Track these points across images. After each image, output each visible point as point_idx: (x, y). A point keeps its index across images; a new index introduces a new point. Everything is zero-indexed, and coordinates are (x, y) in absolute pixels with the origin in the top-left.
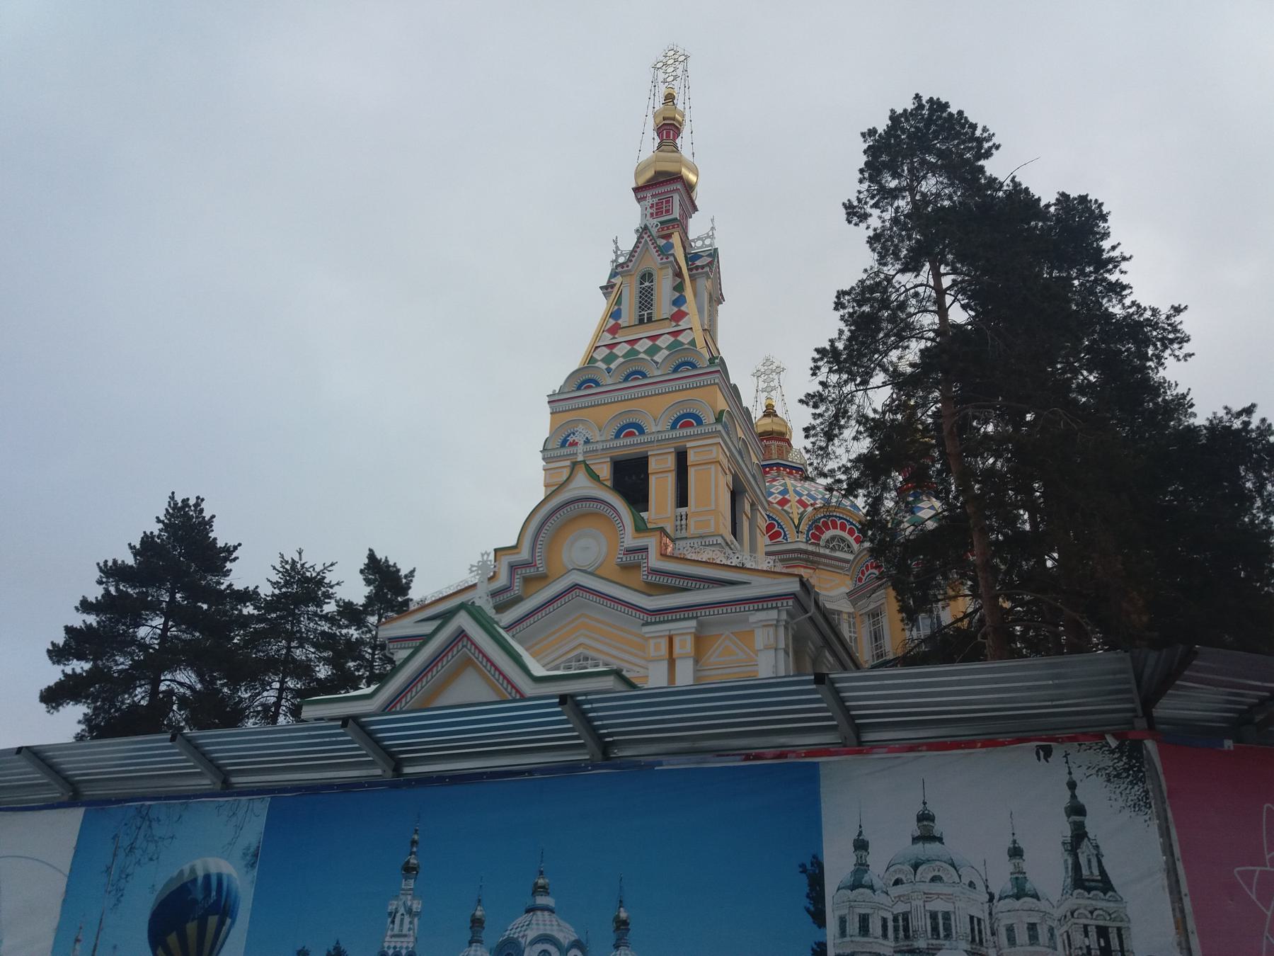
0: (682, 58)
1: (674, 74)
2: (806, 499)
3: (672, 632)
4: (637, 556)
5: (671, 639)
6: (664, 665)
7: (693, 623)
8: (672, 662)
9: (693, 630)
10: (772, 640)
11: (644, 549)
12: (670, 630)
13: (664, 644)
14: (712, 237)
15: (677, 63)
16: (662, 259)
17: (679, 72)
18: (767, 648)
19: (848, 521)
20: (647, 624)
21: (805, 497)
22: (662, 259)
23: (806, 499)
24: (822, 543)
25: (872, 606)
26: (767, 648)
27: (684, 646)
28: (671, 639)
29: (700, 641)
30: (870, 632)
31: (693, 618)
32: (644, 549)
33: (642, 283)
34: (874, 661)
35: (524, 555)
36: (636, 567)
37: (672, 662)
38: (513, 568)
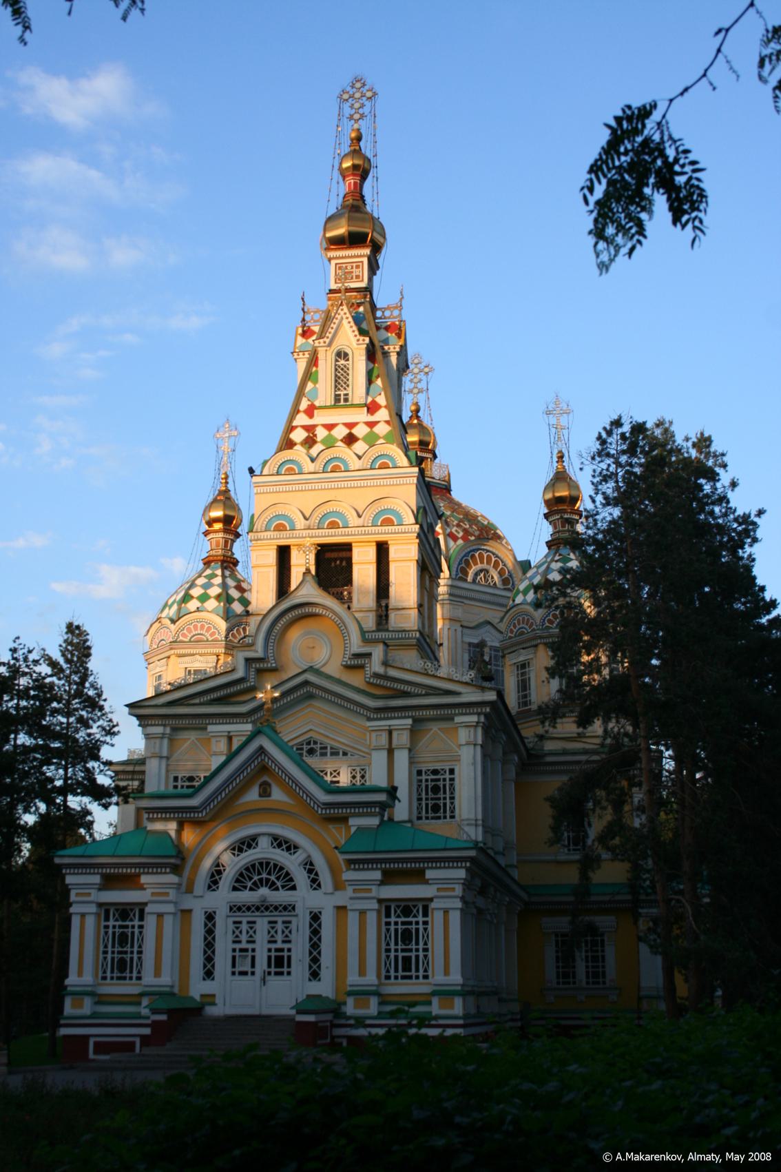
0: (369, 94)
1: (361, 111)
2: (459, 533)
3: (392, 728)
4: (360, 661)
5: (390, 733)
6: (384, 754)
7: (409, 721)
8: (391, 752)
9: (409, 727)
10: (472, 739)
11: (369, 655)
12: (390, 726)
13: (385, 736)
14: (400, 307)
15: (364, 99)
16: (358, 340)
17: (366, 110)
18: (468, 744)
19: (494, 554)
20: (369, 719)
21: (455, 528)
22: (358, 340)
23: (456, 531)
24: (470, 578)
25: (521, 659)
26: (468, 744)
27: (401, 739)
28: (390, 733)
29: (414, 732)
30: (518, 681)
31: (409, 717)
32: (369, 655)
33: (337, 361)
34: (519, 708)
35: (259, 653)
36: (362, 667)
37: (391, 752)
38: (248, 661)
